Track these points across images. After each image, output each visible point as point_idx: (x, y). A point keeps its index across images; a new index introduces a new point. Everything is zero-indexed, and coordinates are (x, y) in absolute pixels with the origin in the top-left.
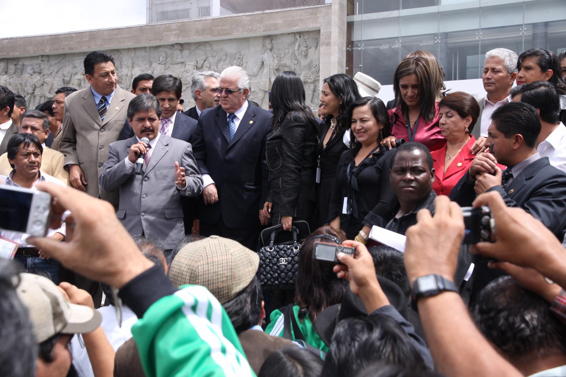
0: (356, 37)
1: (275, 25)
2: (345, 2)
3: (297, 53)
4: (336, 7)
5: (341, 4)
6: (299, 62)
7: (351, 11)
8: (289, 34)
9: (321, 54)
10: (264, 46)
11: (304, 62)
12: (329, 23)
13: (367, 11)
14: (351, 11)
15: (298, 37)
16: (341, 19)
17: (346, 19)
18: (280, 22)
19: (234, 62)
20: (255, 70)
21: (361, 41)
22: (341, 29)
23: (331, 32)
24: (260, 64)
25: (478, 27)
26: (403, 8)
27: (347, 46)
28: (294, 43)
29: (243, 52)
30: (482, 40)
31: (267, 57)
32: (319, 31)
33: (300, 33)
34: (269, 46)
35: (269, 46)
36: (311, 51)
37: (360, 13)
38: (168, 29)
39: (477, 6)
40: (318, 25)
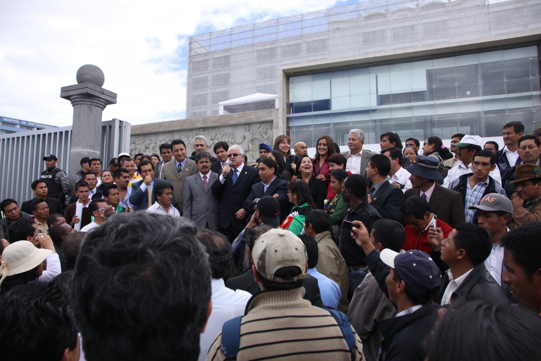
0: (291, 124)
1: (251, 118)
2: (285, 108)
4: (281, 110)
5: (283, 109)
6: (263, 137)
10: (245, 129)
11: (265, 137)
12: (278, 118)
13: (296, 112)
16: (283, 116)
17: (286, 116)
19: (231, 137)
20: (241, 140)
22: (283, 121)
24: (243, 136)
26: (314, 111)
27: (287, 129)
29: (235, 132)
31: (247, 134)
32: (272, 122)
33: (263, 122)
34: (248, 129)
35: (248, 129)
36: (269, 131)
38: (197, 121)
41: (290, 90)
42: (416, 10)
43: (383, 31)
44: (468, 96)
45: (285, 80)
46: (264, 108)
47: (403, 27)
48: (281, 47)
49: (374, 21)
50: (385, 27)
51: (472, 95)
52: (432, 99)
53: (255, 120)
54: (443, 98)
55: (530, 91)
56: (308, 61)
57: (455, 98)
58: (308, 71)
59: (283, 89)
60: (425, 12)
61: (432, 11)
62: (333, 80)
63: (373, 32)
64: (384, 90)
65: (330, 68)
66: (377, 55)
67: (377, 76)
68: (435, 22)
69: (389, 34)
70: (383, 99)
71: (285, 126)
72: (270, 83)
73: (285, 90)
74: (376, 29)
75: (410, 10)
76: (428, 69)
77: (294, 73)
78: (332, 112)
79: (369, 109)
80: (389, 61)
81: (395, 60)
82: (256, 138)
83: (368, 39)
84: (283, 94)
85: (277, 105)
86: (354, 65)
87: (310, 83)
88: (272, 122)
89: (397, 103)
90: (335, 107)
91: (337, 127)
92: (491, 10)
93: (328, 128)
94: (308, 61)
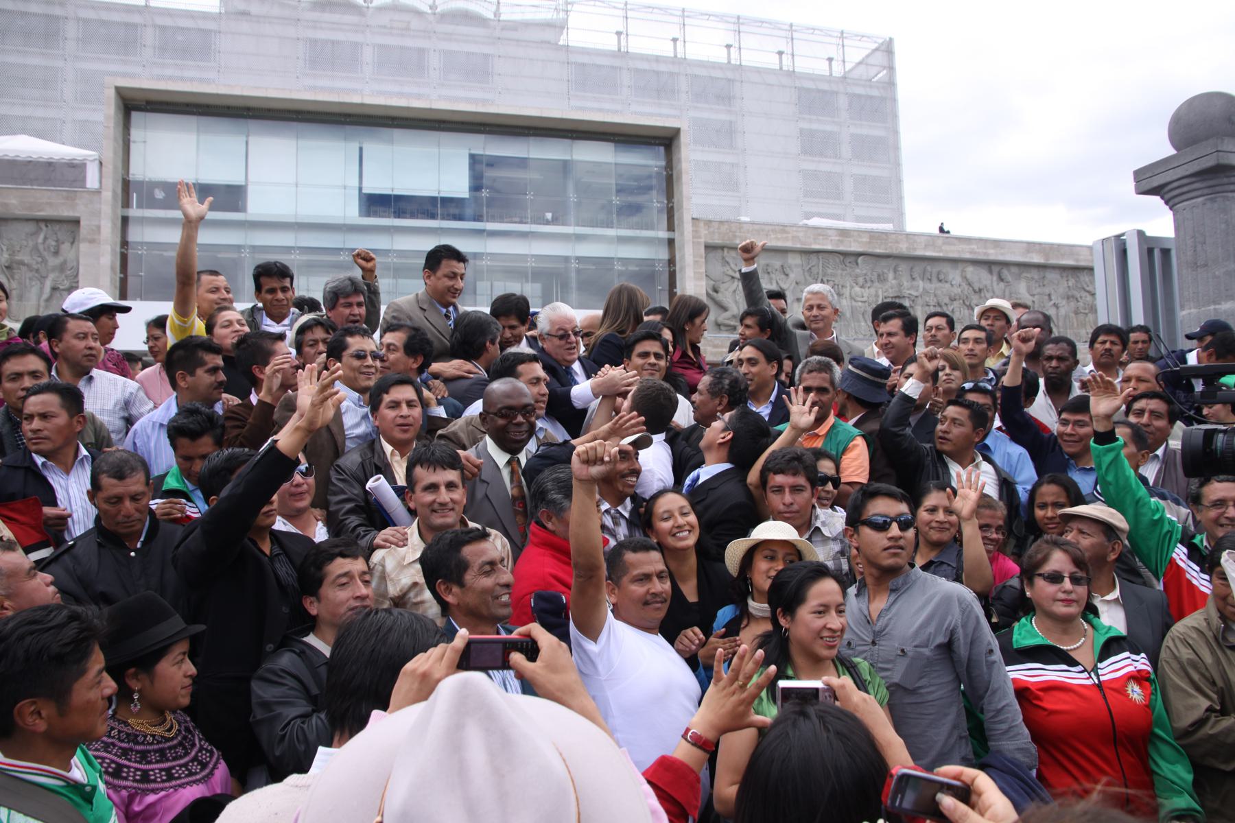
0: (134, 235)
1: (6, 205)
2: (119, 191)
3: (41, 247)
4: (107, 195)
5: (114, 192)
6: (44, 261)
7: (126, 203)
8: (28, 220)
9: (81, 255)
11: (53, 262)
12: (97, 214)
14: (126, 203)
15: (43, 225)
16: (114, 212)
17: (120, 212)
18: (14, 201)
21: (142, 243)
22: (114, 224)
23: (99, 227)
25: (292, 244)
28: (36, 233)
32: (76, 222)
33: (47, 221)
36: (65, 247)
37: (140, 206)
40: (77, 214)
41: (132, 146)
42: (431, 18)
43: (356, 46)
44: (547, 223)
45: (121, 116)
46: (48, 181)
47: (402, 48)
48: (78, 19)
49: (336, 17)
50: (358, 38)
52: (478, 218)
53: (20, 212)
54: (501, 219)
55: (652, 228)
56: (161, 78)
57: (521, 222)
58: (188, 105)
59: (115, 140)
60: (449, 28)
61: (463, 29)
62: (252, 139)
63: (333, 42)
64: (377, 184)
65: (248, 109)
66: (369, 100)
67: (361, 149)
68: (468, 54)
69: (368, 55)
70: (375, 203)
71: (118, 240)
72: (40, 113)
73: (121, 142)
74: (340, 36)
75: (418, 13)
76: (473, 152)
77: (148, 102)
78: (249, 218)
79: (341, 222)
80: (393, 119)
81: (407, 119)
82: (22, 263)
83: (321, 55)
84: (115, 153)
85: (92, 181)
86: (309, 112)
87: (194, 137)
88: (76, 222)
90: (258, 206)
91: (257, 256)
92: (574, 58)
94: (161, 78)
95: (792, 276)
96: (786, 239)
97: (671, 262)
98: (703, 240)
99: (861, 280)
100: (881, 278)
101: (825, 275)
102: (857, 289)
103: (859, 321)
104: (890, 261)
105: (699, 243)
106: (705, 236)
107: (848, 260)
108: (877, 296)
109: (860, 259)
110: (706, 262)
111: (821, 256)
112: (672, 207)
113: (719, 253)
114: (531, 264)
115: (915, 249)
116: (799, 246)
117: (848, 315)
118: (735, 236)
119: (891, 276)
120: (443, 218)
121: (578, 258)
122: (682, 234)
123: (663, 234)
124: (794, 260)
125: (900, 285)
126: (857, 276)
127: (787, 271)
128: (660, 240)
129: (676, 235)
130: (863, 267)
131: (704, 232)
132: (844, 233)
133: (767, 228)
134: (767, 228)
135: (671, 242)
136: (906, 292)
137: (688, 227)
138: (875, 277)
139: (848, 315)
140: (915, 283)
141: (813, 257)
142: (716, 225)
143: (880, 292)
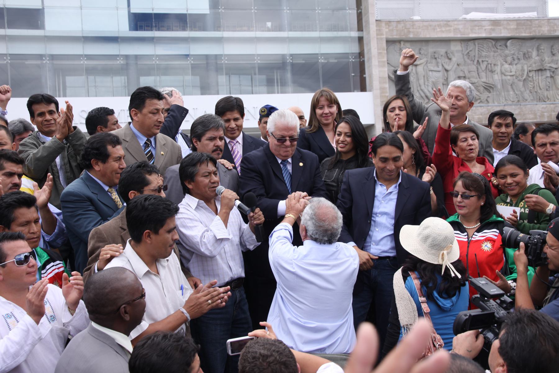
26: (10, 27)
30: (86, 64)
39: (81, 35)
44: (269, 30)
51: (273, 29)
52: (217, 28)
57: (249, 30)
78: (47, 34)
89: (147, 30)
90: (53, 24)
91: (55, 62)
93: (39, 62)
95: (454, 59)
96: (449, 31)
97: (361, 54)
98: (385, 36)
99: (509, 59)
100: (527, 56)
101: (480, 56)
102: (506, 66)
103: (508, 91)
104: (534, 42)
105: (382, 39)
106: (387, 33)
107: (499, 44)
108: (523, 70)
109: (509, 43)
110: (388, 53)
111: (477, 42)
112: (361, 13)
113: (397, 46)
114: (258, 61)
115: (555, 31)
116: (459, 36)
117: (499, 86)
118: (409, 32)
119: (534, 53)
120: (191, 30)
121: (291, 55)
122: (369, 33)
123: (355, 34)
124: (456, 48)
125: (542, 61)
126: (506, 56)
127: (450, 56)
128: (352, 38)
129: (364, 34)
130: (511, 49)
131: (385, 30)
132: (495, 23)
133: (434, 24)
134: (434, 24)
135: (360, 40)
136: (547, 66)
137: (373, 28)
138: (521, 56)
139: (499, 86)
140: (555, 58)
141: (471, 45)
142: (394, 24)
143: (525, 67)
